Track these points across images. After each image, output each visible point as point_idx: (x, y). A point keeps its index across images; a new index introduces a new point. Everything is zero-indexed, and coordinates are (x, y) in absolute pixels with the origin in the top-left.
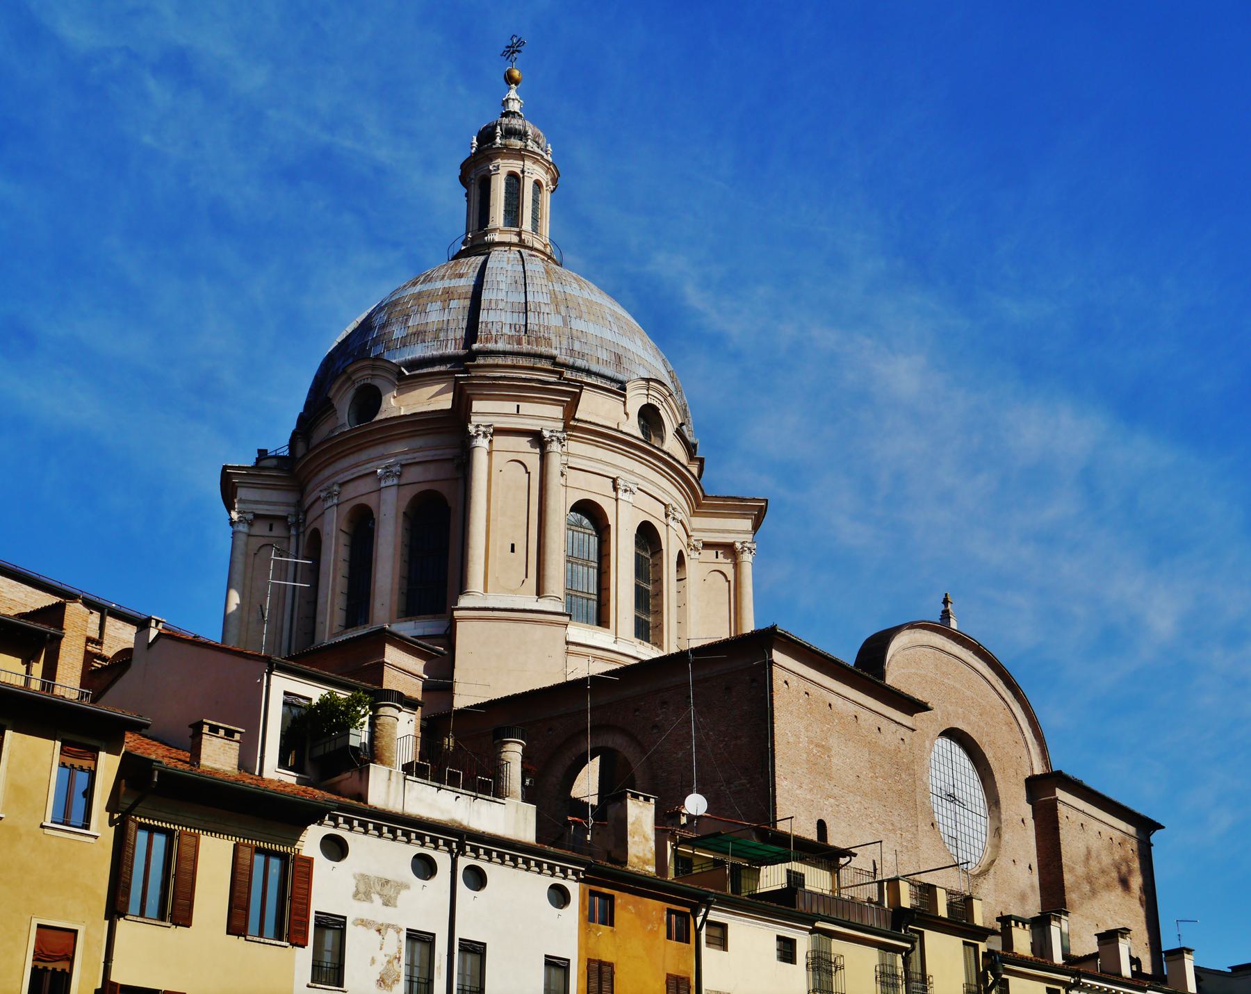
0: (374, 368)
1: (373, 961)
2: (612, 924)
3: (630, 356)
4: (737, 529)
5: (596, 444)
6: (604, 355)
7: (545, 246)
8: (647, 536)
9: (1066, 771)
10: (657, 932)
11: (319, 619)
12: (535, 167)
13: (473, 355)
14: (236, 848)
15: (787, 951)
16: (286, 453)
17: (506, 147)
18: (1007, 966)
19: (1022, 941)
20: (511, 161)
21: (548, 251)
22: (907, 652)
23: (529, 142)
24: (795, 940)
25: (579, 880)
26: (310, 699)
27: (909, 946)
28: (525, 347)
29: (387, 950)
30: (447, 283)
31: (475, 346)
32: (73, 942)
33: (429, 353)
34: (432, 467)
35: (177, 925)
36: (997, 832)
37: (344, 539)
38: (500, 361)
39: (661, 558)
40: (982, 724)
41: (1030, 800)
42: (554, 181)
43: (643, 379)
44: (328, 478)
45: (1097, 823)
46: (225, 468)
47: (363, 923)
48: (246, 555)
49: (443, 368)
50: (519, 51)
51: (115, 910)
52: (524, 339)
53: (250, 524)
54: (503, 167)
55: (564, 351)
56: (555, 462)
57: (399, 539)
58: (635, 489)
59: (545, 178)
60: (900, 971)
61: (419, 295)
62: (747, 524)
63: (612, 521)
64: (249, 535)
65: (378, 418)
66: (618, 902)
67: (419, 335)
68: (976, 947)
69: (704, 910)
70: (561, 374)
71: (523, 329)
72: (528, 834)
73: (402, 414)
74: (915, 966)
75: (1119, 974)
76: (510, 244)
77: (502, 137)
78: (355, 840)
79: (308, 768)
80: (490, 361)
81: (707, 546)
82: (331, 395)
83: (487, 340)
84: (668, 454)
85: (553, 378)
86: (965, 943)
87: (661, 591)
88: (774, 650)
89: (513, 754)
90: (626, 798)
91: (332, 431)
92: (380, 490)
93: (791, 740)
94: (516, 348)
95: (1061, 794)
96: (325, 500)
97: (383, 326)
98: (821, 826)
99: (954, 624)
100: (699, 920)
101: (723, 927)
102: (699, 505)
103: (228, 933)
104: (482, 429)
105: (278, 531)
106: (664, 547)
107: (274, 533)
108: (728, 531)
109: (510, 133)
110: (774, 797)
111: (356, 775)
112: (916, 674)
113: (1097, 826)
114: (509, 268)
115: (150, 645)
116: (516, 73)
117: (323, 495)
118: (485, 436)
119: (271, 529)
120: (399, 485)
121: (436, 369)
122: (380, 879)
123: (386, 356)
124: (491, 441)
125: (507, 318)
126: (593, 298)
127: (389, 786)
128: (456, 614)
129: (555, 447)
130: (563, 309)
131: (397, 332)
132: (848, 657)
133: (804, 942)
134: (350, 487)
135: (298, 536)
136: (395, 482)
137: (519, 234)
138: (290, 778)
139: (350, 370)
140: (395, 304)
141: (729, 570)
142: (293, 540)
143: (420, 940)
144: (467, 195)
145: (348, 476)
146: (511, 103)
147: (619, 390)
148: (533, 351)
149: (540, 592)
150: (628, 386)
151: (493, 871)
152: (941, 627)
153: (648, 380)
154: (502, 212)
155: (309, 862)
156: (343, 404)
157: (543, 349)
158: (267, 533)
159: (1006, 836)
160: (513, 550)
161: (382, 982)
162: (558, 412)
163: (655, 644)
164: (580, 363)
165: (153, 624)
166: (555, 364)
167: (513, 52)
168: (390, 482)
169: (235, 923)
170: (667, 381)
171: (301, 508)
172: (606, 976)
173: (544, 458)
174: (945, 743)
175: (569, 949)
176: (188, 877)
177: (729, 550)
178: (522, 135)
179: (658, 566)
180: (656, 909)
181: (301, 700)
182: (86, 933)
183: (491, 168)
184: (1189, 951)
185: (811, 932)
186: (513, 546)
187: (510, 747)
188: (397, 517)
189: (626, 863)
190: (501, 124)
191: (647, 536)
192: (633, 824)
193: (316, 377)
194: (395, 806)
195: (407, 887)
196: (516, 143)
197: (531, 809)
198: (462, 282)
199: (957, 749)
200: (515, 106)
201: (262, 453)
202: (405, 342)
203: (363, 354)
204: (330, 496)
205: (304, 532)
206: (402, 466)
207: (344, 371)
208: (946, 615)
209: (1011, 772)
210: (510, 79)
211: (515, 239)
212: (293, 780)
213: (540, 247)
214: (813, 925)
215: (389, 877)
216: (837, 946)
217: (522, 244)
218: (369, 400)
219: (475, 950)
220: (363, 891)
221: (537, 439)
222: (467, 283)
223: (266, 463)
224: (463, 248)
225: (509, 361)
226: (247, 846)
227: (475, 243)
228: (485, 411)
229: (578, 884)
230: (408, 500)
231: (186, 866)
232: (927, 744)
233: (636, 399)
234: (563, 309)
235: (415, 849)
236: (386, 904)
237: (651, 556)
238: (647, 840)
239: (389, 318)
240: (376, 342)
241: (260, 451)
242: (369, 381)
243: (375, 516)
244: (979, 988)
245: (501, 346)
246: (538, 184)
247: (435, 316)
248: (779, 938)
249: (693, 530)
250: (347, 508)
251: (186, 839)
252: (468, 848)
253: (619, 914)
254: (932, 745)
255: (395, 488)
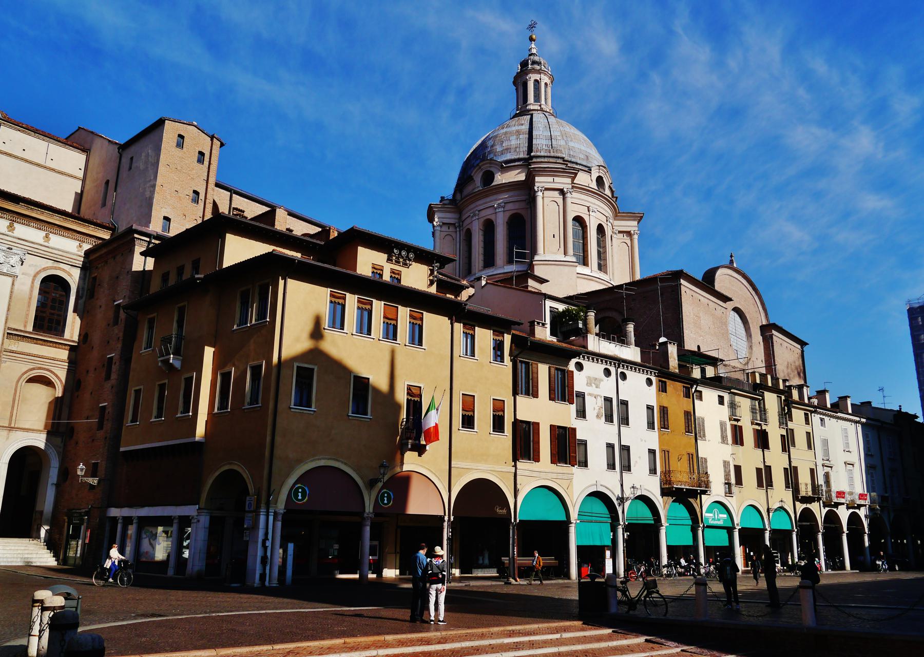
0: (490, 163)
1: (594, 409)
2: (666, 392)
3: (591, 156)
4: (631, 225)
5: (581, 193)
6: (582, 156)
7: (550, 110)
8: (600, 229)
9: (777, 323)
10: (680, 395)
11: (473, 264)
12: (545, 77)
13: (531, 158)
14: (549, 368)
15: (721, 400)
16: (451, 198)
17: (533, 69)
18: (794, 405)
19: (795, 394)
20: (536, 75)
21: (551, 112)
22: (721, 277)
23: (542, 67)
24: (723, 397)
25: (656, 376)
26: (557, 309)
27: (761, 398)
28: (552, 154)
29: (598, 405)
30: (517, 128)
31: (532, 154)
32: (503, 405)
33: (513, 157)
34: (517, 204)
35: (534, 397)
36: (751, 347)
37: (481, 233)
38: (542, 160)
39: (605, 238)
40: (745, 305)
41: (762, 335)
42: (552, 82)
43: (598, 166)
44: (472, 209)
45: (786, 343)
46: (431, 204)
47: (590, 394)
48: (440, 239)
49: (519, 163)
50: (535, 27)
51: (515, 393)
52: (552, 150)
53: (441, 227)
54: (532, 77)
55: (567, 155)
56: (569, 201)
57: (505, 232)
58: (596, 211)
59: (548, 81)
60: (757, 407)
61: (506, 133)
62: (635, 223)
63: (588, 224)
64: (441, 231)
65: (494, 184)
66: (668, 384)
67: (508, 150)
68: (781, 397)
69: (695, 386)
70: (567, 164)
71: (551, 146)
72: (638, 359)
73: (504, 182)
74: (762, 406)
75: (827, 407)
76: (537, 110)
77: (532, 64)
78: (585, 363)
79: (559, 334)
80: (539, 160)
81: (620, 232)
82: (472, 175)
83: (537, 151)
84: (607, 196)
85: (564, 167)
86: (778, 396)
87: (606, 251)
88: (681, 280)
89: (631, 328)
90: (667, 344)
91: (474, 189)
92: (496, 213)
93: (688, 314)
94: (549, 154)
95: (774, 332)
96: (472, 217)
97: (492, 146)
98: (699, 347)
99: (735, 265)
100: (693, 390)
101: (701, 392)
102: (616, 216)
103: (550, 400)
104: (540, 188)
105: (452, 229)
106: (606, 234)
107: (450, 230)
108: (629, 226)
109: (534, 63)
110: (683, 337)
111: (581, 339)
112: (723, 286)
113: (786, 344)
114: (542, 121)
115: (483, 287)
116: (534, 37)
117: (471, 215)
118: (541, 191)
119: (449, 229)
120: (504, 211)
121: (516, 164)
122: (594, 378)
123: (495, 158)
124: (543, 193)
125: (544, 142)
126: (576, 133)
127: (594, 343)
128: (534, 263)
129: (568, 195)
130: (565, 137)
131: (498, 149)
132: (699, 277)
133: (727, 397)
134: (483, 211)
135: (460, 231)
136: (502, 209)
137: (540, 106)
138: (554, 339)
139: (480, 164)
140: (496, 137)
141: (629, 242)
142: (458, 233)
143: (608, 400)
144: (516, 89)
145: (482, 207)
146: (533, 50)
147: (589, 170)
148: (555, 156)
149: (565, 253)
150: (592, 169)
151: (628, 373)
152: (730, 266)
153: (599, 166)
154: (533, 97)
155: (572, 372)
156: (478, 178)
157: (559, 155)
158: (448, 230)
159: (754, 349)
160: (554, 237)
161: (598, 416)
162: (569, 180)
163: (604, 272)
164: (573, 160)
165: (483, 279)
166: (564, 161)
167: (532, 28)
168: (500, 210)
169: (552, 396)
170: (606, 167)
171: (461, 221)
172: (666, 412)
173: (564, 199)
174: (732, 313)
175: (654, 403)
176: (536, 380)
177: (629, 233)
178: (539, 63)
179: (604, 241)
180: (679, 385)
181: (555, 309)
182: (507, 401)
183: (527, 78)
184: (849, 397)
185: (729, 393)
186: (554, 235)
187: (630, 326)
188: (504, 224)
189: (669, 369)
190: (530, 59)
191: (600, 229)
192: (671, 354)
193: (462, 167)
194: (596, 350)
195: (602, 381)
196: (537, 67)
197: (638, 349)
198: (523, 127)
199: (736, 314)
200: (534, 51)
201: (443, 198)
202: (502, 153)
203: (484, 158)
204: (475, 215)
205: (462, 230)
206: (505, 203)
207: (478, 165)
208: (732, 262)
209: (755, 323)
210: (531, 39)
211: (539, 108)
212: (556, 340)
213: (548, 111)
214: (730, 390)
215: (597, 377)
216: (737, 398)
217: (542, 110)
218: (489, 177)
219: (625, 404)
220: (589, 384)
221: (562, 192)
222: (526, 127)
223: (445, 202)
224: (517, 112)
225: (546, 160)
226: (553, 367)
227: (522, 110)
228: (541, 181)
229: (655, 377)
230: (508, 217)
231: (535, 375)
232: (728, 313)
233: (595, 174)
234: (565, 137)
235: (604, 366)
236: (597, 387)
237: (601, 237)
238: (675, 359)
239: (494, 143)
240: (490, 153)
241: (441, 197)
242: (489, 169)
243: (495, 223)
244: (782, 413)
245: (542, 154)
246: (546, 84)
247: (514, 142)
248: (719, 396)
249: (614, 226)
250: (482, 220)
251: (534, 365)
252: (621, 365)
253: (668, 388)
254: (730, 312)
255: (502, 213)
